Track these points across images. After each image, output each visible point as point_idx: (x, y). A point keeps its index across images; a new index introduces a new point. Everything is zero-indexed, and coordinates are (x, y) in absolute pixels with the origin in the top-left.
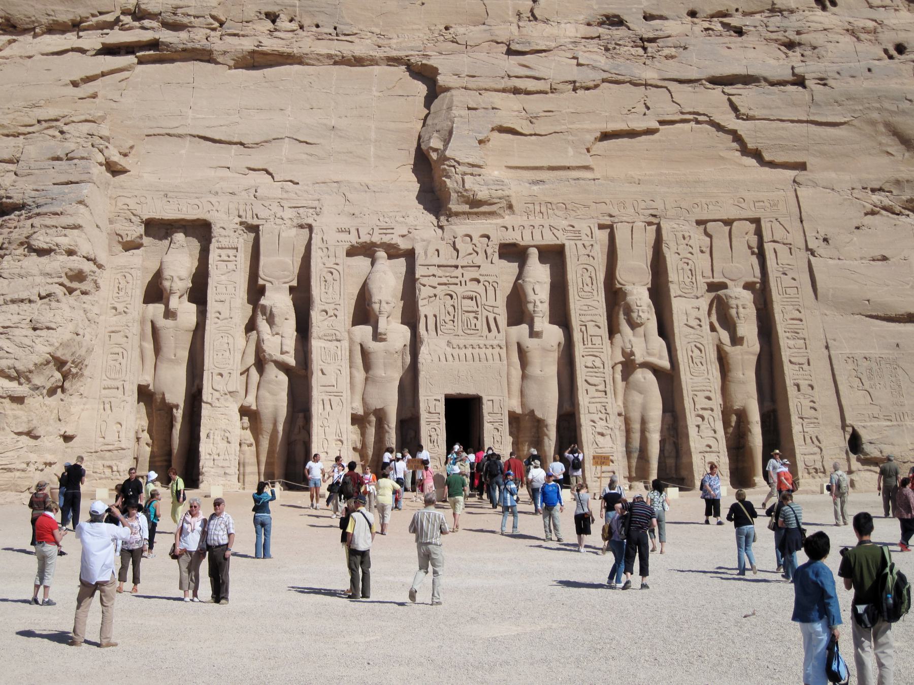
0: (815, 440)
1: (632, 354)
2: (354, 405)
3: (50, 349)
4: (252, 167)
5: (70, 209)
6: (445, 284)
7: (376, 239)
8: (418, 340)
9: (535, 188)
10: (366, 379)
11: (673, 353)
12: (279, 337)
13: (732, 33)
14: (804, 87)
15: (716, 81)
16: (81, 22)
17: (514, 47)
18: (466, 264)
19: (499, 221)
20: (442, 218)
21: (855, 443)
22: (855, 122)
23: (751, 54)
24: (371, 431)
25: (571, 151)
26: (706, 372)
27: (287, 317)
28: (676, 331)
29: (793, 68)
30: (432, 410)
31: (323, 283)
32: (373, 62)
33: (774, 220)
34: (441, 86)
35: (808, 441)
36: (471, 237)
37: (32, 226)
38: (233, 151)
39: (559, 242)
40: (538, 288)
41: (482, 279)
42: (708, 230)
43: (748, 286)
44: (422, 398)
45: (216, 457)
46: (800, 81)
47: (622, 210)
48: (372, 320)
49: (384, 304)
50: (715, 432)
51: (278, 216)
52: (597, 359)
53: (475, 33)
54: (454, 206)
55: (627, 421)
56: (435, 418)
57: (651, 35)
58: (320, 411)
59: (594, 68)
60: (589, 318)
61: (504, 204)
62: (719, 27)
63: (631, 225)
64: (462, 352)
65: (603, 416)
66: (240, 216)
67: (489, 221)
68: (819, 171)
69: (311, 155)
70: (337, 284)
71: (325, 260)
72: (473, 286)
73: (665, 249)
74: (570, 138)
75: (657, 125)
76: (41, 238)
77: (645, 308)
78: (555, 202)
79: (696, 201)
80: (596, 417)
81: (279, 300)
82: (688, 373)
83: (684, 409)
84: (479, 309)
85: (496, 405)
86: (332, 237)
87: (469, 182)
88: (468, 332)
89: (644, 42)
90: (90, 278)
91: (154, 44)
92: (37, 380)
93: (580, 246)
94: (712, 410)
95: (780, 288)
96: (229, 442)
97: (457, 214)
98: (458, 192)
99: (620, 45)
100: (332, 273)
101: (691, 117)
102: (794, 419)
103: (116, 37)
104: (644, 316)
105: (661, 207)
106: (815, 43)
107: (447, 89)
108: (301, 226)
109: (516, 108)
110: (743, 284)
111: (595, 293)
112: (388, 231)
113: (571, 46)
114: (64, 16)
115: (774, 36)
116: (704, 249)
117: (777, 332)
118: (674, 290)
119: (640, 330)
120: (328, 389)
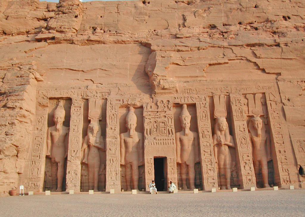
0: (287, 170)
1: (221, 141)
3: (12, 142)
4: (86, 79)
5: (21, 93)
8: (144, 137)
9: (185, 84)
13: (254, 29)
14: (280, 47)
15: (248, 45)
16: (29, 31)
17: (178, 36)
18: (161, 111)
19: (172, 95)
20: (153, 95)
21: (301, 171)
22: (298, 58)
23: (260, 36)
24: (128, 170)
28: (236, 132)
29: (275, 40)
30: (149, 162)
31: (110, 118)
32: (129, 42)
33: (270, 93)
34: (152, 50)
35: (284, 171)
36: (163, 101)
37: (7, 100)
38: (80, 73)
39: (194, 102)
40: (186, 118)
42: (247, 97)
43: (261, 116)
44: (145, 158)
45: (72, 180)
46: (278, 45)
48: (128, 131)
49: (132, 125)
50: (250, 168)
51: (95, 95)
52: (208, 143)
53: (165, 32)
54: (156, 91)
55: (219, 165)
57: (226, 31)
58: (109, 163)
59: (206, 42)
61: (175, 90)
62: (249, 28)
66: (82, 96)
68: (285, 75)
69: (107, 74)
71: (111, 110)
72: (163, 119)
73: (231, 104)
74: (197, 66)
75: (227, 61)
76: (10, 104)
77: (225, 125)
79: (243, 87)
80: (208, 164)
81: (95, 125)
82: (240, 148)
85: (172, 160)
87: (162, 82)
89: (222, 33)
90: (28, 118)
91: (53, 38)
92: (7, 153)
93: (201, 103)
94: (249, 160)
95: (273, 117)
96: (76, 174)
97: (158, 93)
98: (158, 86)
99: (214, 34)
100: (114, 115)
101: (240, 58)
102: (279, 163)
103: (40, 36)
106: (283, 32)
107: (154, 51)
109: (178, 56)
110: (260, 116)
112: (134, 100)
113: (197, 35)
114: (24, 30)
115: (269, 30)
116: (245, 103)
117: (272, 132)
118: (235, 118)
119: (223, 132)
120: (112, 155)
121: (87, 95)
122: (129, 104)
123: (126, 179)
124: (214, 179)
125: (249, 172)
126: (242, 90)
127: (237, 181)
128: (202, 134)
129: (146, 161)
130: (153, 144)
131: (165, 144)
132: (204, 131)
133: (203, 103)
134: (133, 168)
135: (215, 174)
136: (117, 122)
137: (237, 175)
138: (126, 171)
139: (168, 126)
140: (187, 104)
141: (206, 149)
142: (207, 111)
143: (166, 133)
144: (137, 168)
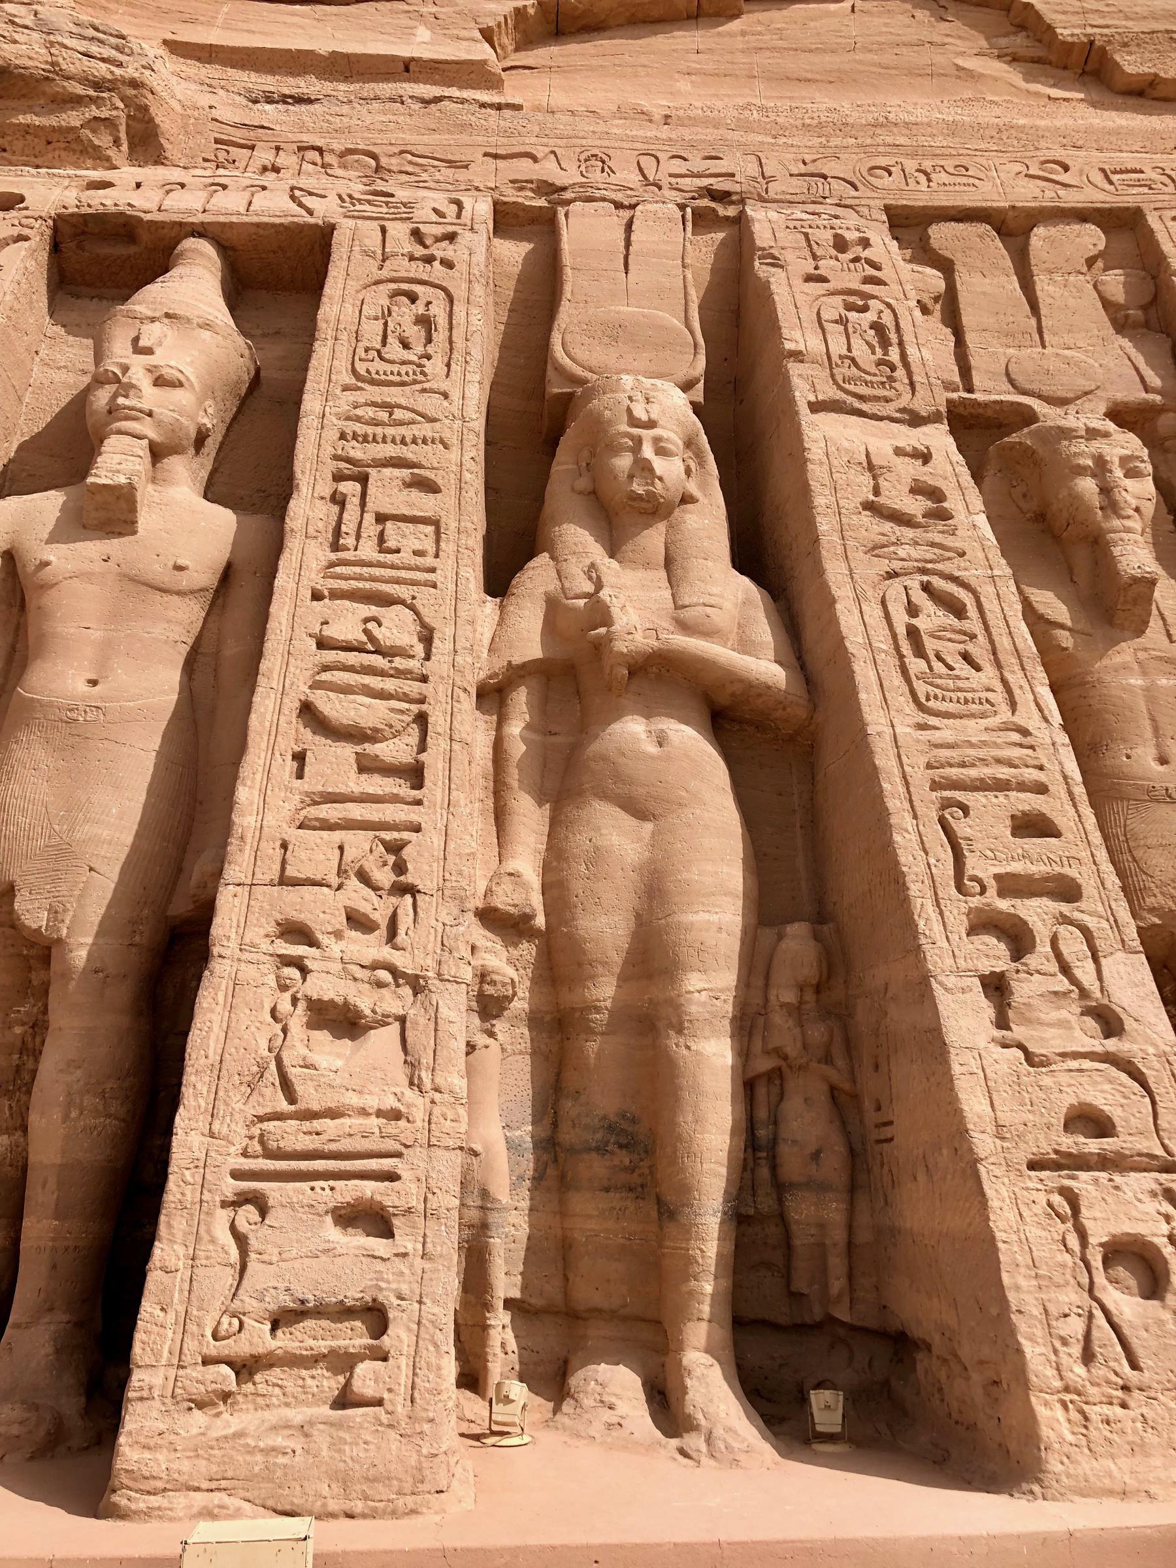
11: (811, 632)
25: (423, 33)
26: (999, 697)
28: (825, 525)
42: (935, 243)
47: (597, 176)
50: (1109, 1022)
60: (390, 450)
61: (115, 108)
63: (627, 214)
65: (377, 908)
73: (761, 269)
78: (338, 146)
79: (883, 161)
80: (320, 909)
82: (901, 700)
83: (896, 881)
94: (1067, 891)
104: (670, 469)
105: (753, 169)
110: (1103, 408)
111: (435, 367)
124: (374, 1220)
125: (1106, 1092)
126: (886, 181)
127: (850, 1244)
128: (325, 513)
132: (363, 480)
133: (417, 235)
135: (477, 1113)
137: (852, 1152)
140: (221, 236)
141: (346, 690)
142: (459, 293)
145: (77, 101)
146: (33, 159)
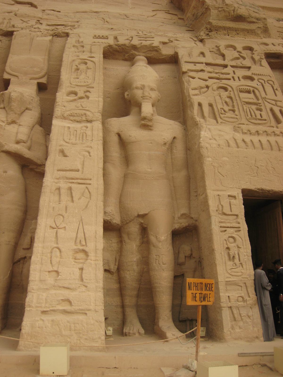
2: (109, 209)
6: (218, 79)
7: (136, 42)
10: (125, 176)
12: (16, 126)
27: (29, 106)
30: (227, 210)
41: (256, 77)
44: (211, 193)
49: (147, 89)
56: (231, 221)
61: (261, 25)
64: (255, 139)
67: (247, 39)
70: (90, 73)
84: (260, 101)
86: (88, 40)
88: (253, 121)
97: (217, 29)
100: (86, 63)
108: (57, 35)
121: (11, 25)
122: (134, 47)
123: (120, 281)
129: (213, 204)
130: (232, 143)
131: (275, 147)
134: (152, 239)
136: (96, 79)
138: (120, 251)
139: (268, 100)
143: (264, 117)
144: (170, 237)
145: (254, 22)
146: (244, 37)
